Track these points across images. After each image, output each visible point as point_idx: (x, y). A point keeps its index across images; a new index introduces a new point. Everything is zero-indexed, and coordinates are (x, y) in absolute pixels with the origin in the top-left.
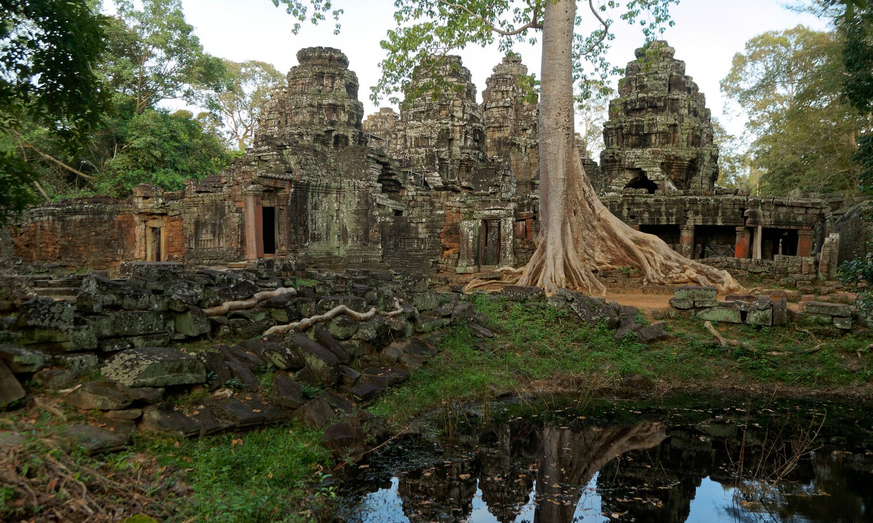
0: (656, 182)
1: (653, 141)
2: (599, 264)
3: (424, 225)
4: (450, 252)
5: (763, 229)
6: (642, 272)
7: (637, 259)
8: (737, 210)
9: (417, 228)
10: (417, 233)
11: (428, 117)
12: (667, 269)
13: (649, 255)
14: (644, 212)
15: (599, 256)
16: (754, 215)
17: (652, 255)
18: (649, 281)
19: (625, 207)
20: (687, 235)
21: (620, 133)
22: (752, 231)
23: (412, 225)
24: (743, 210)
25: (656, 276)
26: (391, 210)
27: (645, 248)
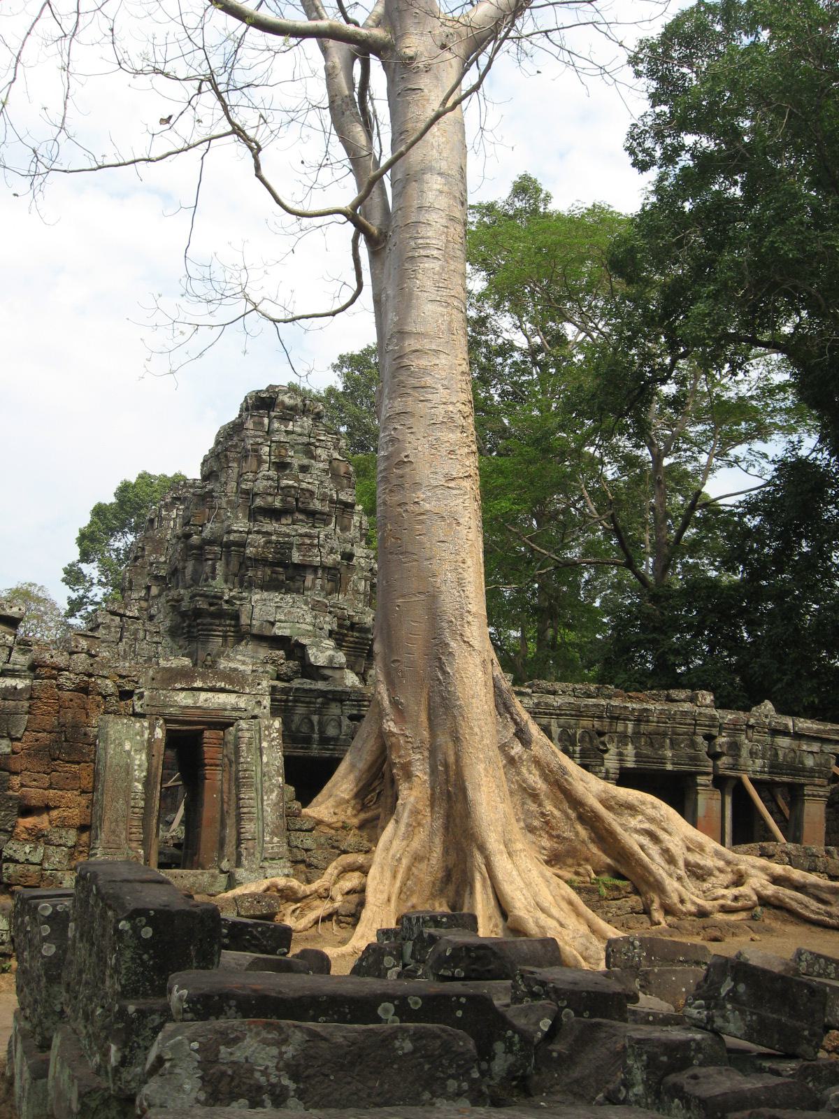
1: (308, 583)
4: (42, 822)
24: (709, 738)
25: (687, 895)
27: (634, 822)
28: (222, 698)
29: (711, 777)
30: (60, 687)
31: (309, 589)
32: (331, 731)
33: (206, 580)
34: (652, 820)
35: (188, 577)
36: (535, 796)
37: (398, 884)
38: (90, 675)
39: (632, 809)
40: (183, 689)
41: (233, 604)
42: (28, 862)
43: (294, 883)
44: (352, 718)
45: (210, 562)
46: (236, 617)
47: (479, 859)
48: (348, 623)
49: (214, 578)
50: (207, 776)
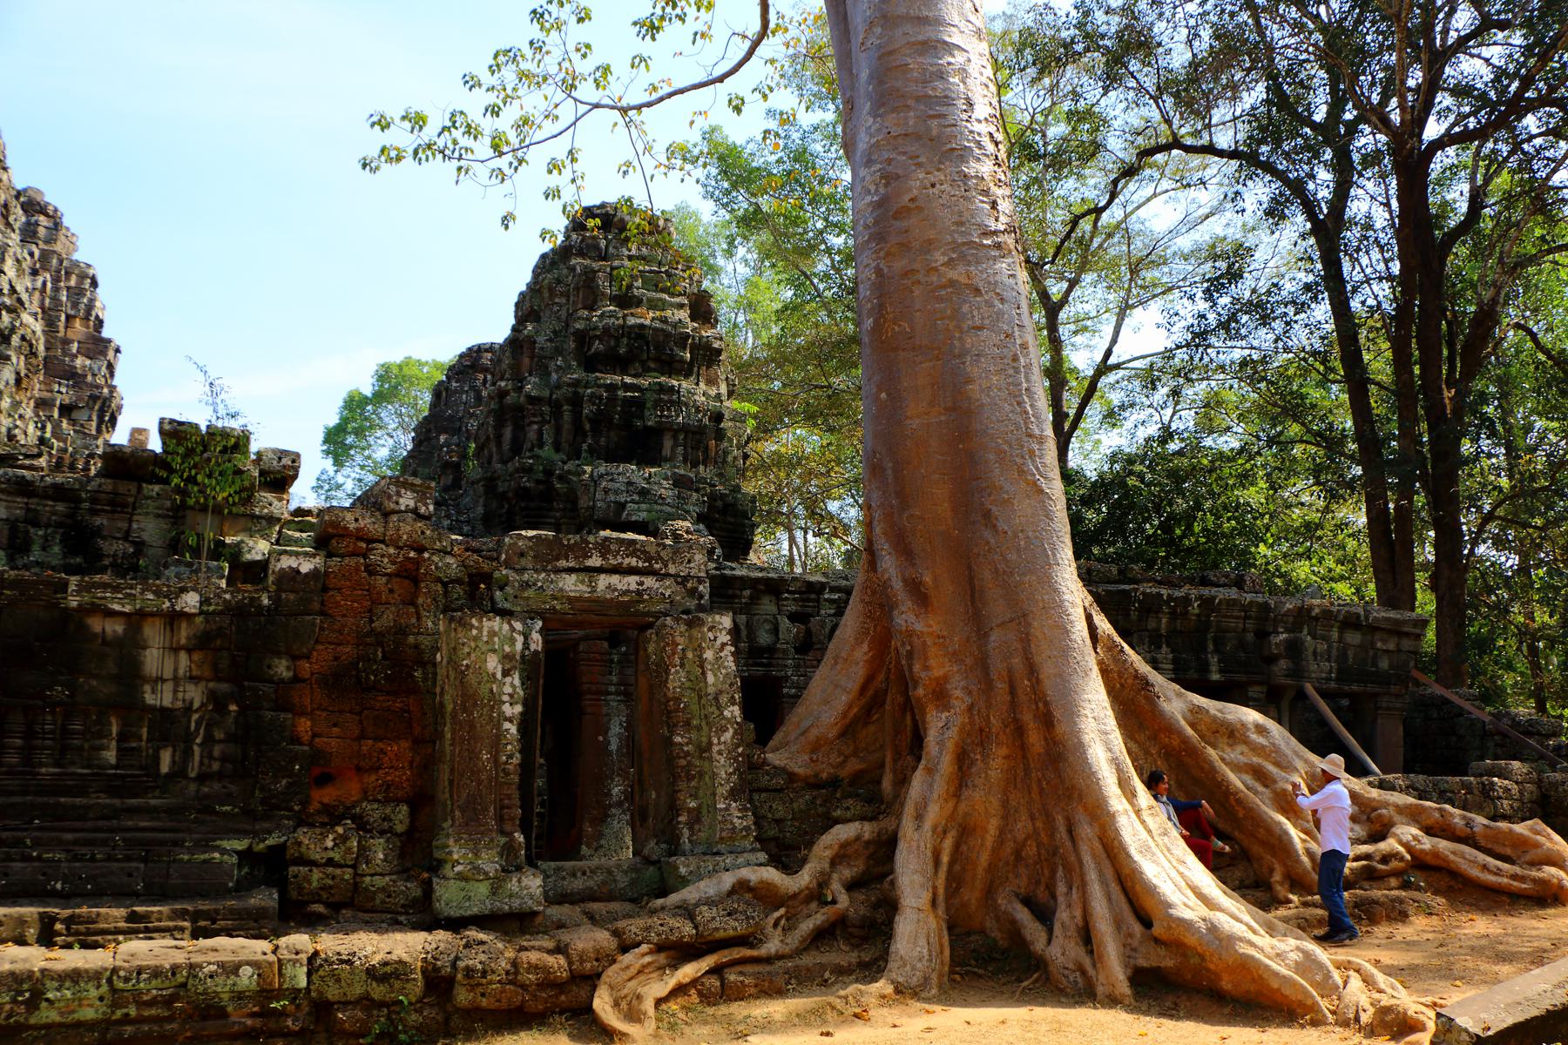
1: (667, 451)
3: (184, 633)
8: (1250, 637)
9: (131, 645)
10: (131, 675)
21: (567, 417)
23: (96, 624)
24: (1263, 635)
27: (1237, 754)
28: (632, 581)
29: (1264, 689)
30: (371, 570)
31: (666, 460)
32: (764, 638)
33: (531, 450)
35: (506, 447)
37: (942, 874)
38: (420, 549)
39: (1232, 734)
40: (570, 570)
41: (568, 482)
42: (330, 862)
43: (771, 874)
44: (793, 617)
45: (536, 427)
46: (573, 500)
47: (1086, 831)
48: (719, 503)
49: (541, 446)
50: (589, 710)
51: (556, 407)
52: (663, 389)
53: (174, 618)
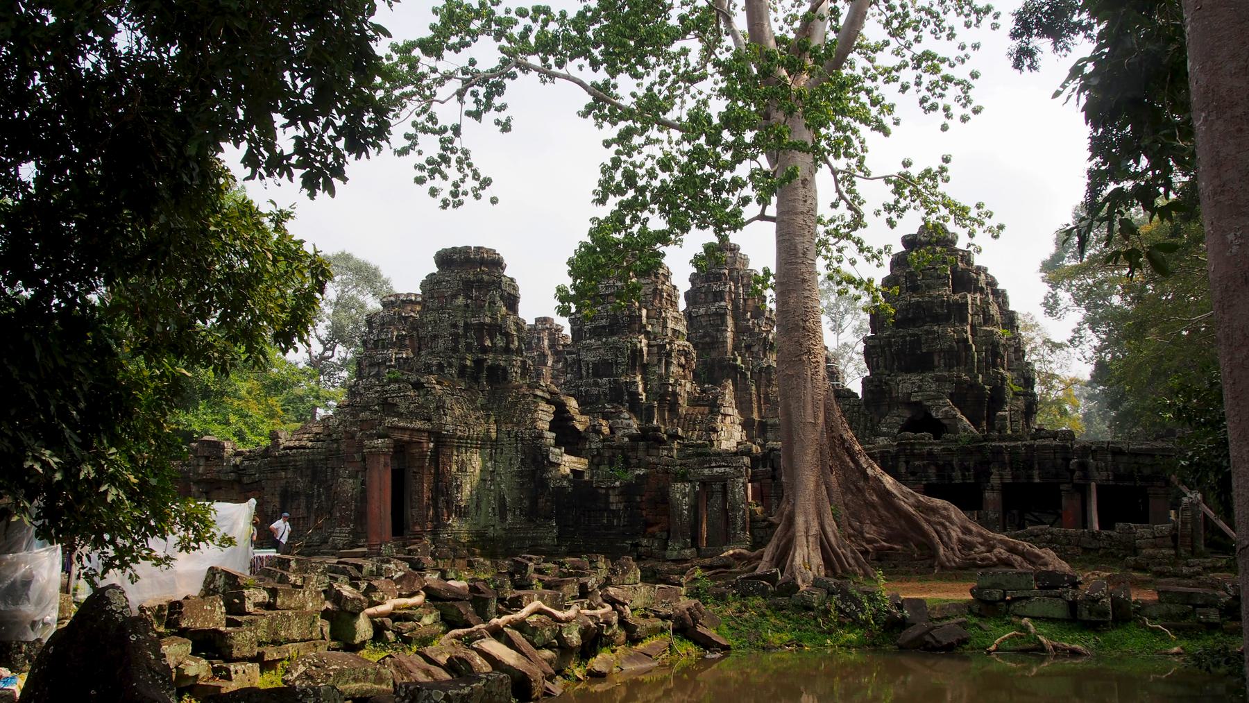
0: (945, 422)
1: (936, 363)
2: (869, 541)
4: (655, 529)
5: (1099, 488)
6: (933, 554)
7: (925, 534)
8: (1059, 461)
9: (607, 495)
10: (608, 503)
11: (612, 333)
12: (966, 546)
13: (939, 528)
14: (929, 465)
15: (870, 532)
16: (1083, 466)
17: (945, 528)
18: (943, 567)
19: (902, 459)
20: (991, 496)
22: (1083, 491)
24: (1067, 460)
26: (568, 471)
27: (933, 519)
34: (943, 517)
36: (874, 507)
39: (934, 510)
51: (882, 347)
52: (928, 332)
53: (615, 488)
